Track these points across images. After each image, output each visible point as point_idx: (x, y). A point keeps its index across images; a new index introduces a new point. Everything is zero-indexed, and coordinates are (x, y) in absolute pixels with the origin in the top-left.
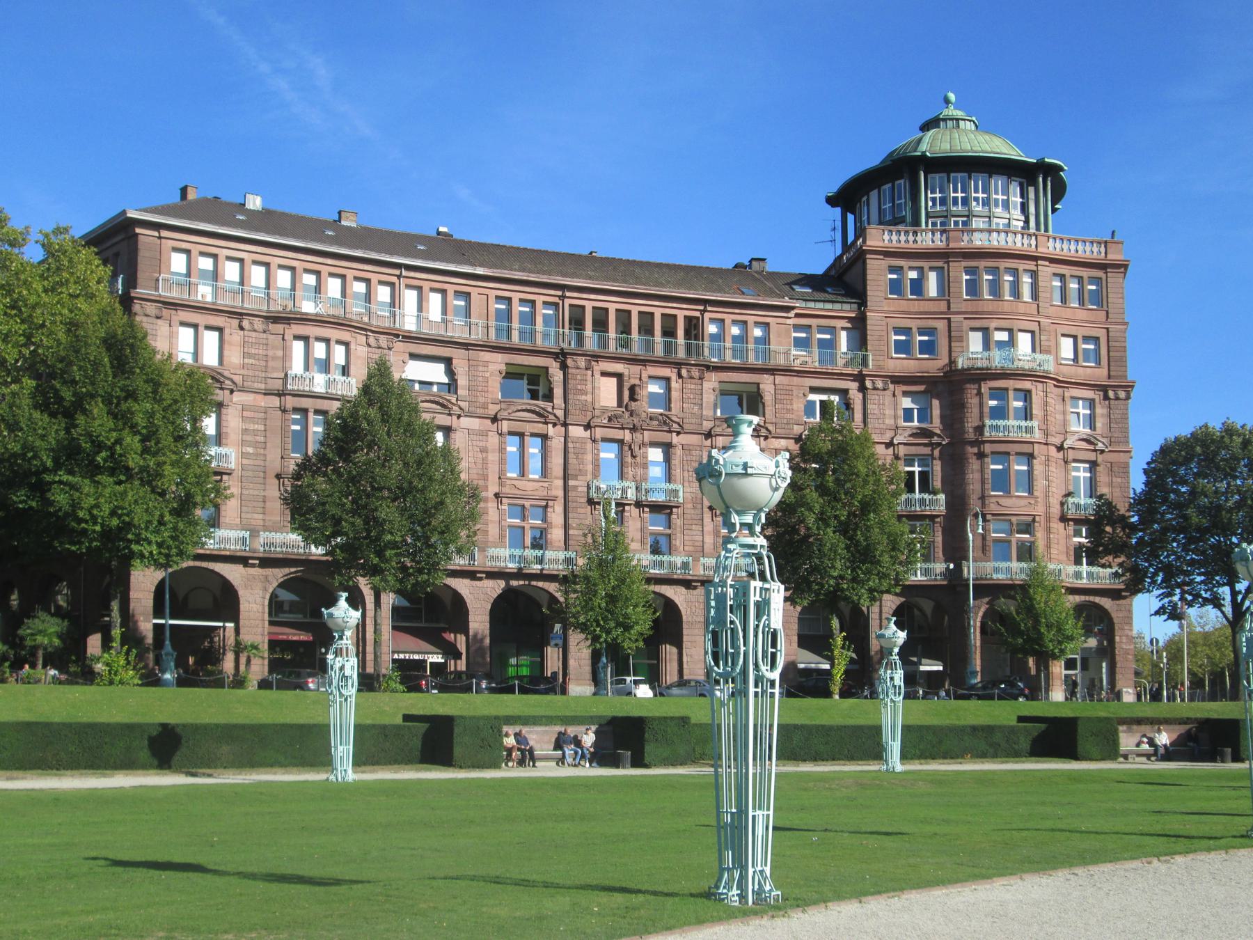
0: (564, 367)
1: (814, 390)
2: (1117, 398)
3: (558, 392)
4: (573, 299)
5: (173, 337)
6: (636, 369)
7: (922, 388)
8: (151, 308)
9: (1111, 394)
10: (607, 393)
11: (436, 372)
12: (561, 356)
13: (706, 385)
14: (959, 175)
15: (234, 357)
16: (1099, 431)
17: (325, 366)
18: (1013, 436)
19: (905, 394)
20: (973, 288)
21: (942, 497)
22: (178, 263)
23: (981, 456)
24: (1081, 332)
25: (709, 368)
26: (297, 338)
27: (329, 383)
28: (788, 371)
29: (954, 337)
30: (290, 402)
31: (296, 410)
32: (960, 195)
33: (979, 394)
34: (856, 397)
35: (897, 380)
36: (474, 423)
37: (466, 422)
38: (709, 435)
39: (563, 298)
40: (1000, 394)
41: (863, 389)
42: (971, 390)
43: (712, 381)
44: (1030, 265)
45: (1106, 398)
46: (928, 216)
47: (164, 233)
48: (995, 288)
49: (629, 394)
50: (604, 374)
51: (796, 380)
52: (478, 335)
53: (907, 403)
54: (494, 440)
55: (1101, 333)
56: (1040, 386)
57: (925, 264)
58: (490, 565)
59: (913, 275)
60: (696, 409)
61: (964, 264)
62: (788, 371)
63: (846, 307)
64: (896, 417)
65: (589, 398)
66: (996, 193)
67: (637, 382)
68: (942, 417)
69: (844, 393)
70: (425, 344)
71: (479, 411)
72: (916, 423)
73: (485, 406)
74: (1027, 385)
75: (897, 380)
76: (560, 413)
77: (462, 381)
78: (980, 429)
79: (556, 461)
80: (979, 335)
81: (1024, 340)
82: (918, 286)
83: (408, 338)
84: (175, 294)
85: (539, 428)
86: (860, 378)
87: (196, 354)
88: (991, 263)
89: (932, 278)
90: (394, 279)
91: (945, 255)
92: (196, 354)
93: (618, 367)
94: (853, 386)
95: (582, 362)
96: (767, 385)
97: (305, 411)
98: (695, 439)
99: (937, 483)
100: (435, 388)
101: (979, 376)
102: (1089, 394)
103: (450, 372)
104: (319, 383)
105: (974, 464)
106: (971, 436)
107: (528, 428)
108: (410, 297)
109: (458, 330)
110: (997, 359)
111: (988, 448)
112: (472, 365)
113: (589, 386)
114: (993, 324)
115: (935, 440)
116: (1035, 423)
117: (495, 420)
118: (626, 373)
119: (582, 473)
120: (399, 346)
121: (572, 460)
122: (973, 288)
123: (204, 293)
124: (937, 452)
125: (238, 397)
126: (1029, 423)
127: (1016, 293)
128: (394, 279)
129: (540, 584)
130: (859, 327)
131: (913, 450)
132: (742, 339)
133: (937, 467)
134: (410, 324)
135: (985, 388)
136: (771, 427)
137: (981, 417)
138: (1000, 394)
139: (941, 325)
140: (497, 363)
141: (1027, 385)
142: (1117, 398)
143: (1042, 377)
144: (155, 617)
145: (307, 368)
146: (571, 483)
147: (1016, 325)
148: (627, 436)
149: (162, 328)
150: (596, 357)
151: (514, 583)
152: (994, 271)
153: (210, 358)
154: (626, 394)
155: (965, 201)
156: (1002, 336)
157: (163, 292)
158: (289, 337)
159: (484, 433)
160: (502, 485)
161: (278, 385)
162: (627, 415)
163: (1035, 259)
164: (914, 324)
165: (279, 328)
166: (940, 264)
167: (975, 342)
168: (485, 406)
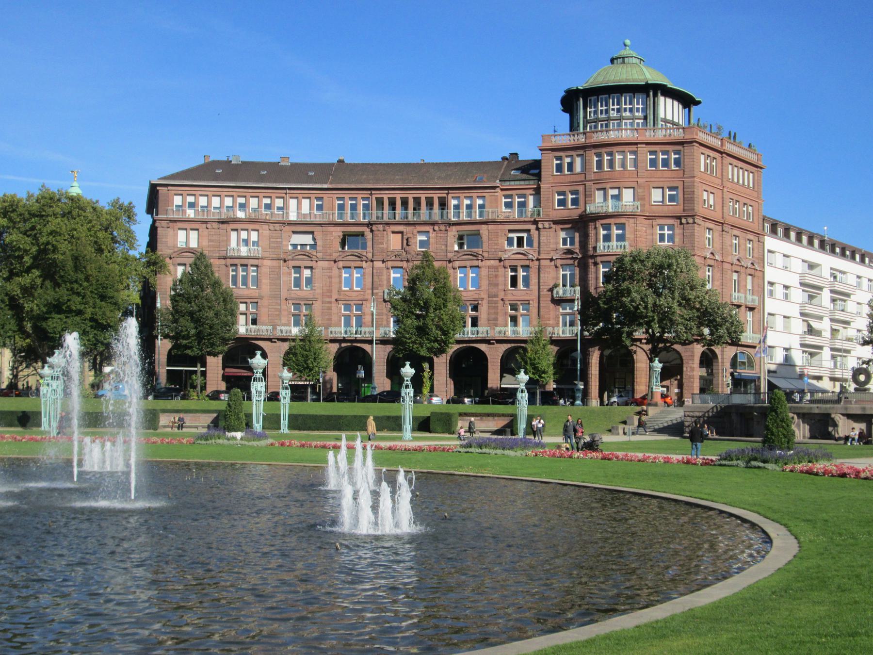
0: (372, 231)
1: (510, 231)
2: (688, 223)
3: (369, 244)
4: (377, 194)
6: (411, 228)
7: (569, 226)
8: (164, 224)
9: (684, 221)
10: (394, 242)
11: (307, 239)
12: (370, 225)
13: (449, 233)
14: (604, 96)
15: (205, 243)
16: (676, 244)
17: (246, 242)
18: (612, 251)
19: (562, 229)
20: (600, 164)
21: (578, 288)
22: (178, 200)
23: (596, 264)
24: (666, 185)
26: (233, 230)
27: (249, 251)
28: (494, 222)
29: (588, 196)
30: (229, 262)
31: (232, 265)
32: (604, 108)
33: (596, 228)
34: (534, 233)
35: (556, 222)
36: (325, 264)
37: (320, 263)
38: (450, 261)
39: (371, 194)
40: (607, 227)
41: (538, 229)
42: (591, 226)
43: (453, 232)
44: (633, 148)
45: (681, 223)
46: (586, 122)
47: (170, 188)
48: (611, 163)
50: (393, 232)
51: (500, 227)
52: (326, 219)
53: (563, 235)
54: (335, 271)
55: (680, 185)
56: (631, 221)
57: (574, 153)
59: (568, 160)
60: (443, 247)
61: (593, 151)
62: (494, 222)
63: (532, 182)
64: (557, 243)
65: (385, 246)
66: (625, 104)
67: (411, 235)
68: (580, 242)
69: (528, 231)
70: (302, 226)
71: (328, 258)
72: (568, 246)
73: (331, 255)
74: (622, 220)
75: (556, 222)
76: (370, 256)
77: (319, 243)
78: (595, 248)
79: (369, 280)
80: (602, 192)
81: (628, 195)
82: (571, 166)
83: (291, 224)
84: (176, 216)
85: (358, 264)
86: (535, 222)
87: (187, 242)
88: (609, 149)
89: (578, 161)
90: (284, 195)
91: (584, 147)
92: (187, 242)
94: (533, 227)
95: (381, 227)
97: (236, 265)
99: (577, 281)
100: (308, 248)
101: (596, 218)
102: (671, 221)
103: (314, 239)
104: (244, 251)
105: (592, 268)
106: (591, 252)
108: (293, 203)
109: (318, 216)
110: (610, 207)
111: (599, 259)
113: (385, 240)
114: (608, 186)
115: (575, 256)
116: (626, 243)
117: (335, 262)
118: (405, 231)
119: (381, 286)
120: (288, 228)
121: (376, 279)
122: (600, 164)
123: (191, 213)
124: (576, 262)
126: (623, 243)
127: (623, 165)
128: (284, 195)
129: (359, 345)
130: (537, 191)
131: (565, 262)
132: (469, 207)
133: (577, 270)
134: (293, 217)
135: (599, 223)
136: (485, 255)
137: (597, 240)
138: (607, 227)
139: (581, 189)
140: (338, 232)
141: (622, 220)
142: (688, 223)
143: (633, 216)
144: (168, 366)
145: (238, 244)
146: (375, 291)
147: (621, 185)
149: (170, 232)
150: (388, 224)
151: (343, 345)
152: (610, 154)
153: (193, 244)
154: (405, 242)
155: (607, 111)
156: (615, 192)
157: (170, 216)
158: (229, 230)
159: (330, 269)
160: (339, 294)
161: (223, 254)
162: (404, 253)
163: (636, 144)
164: (567, 189)
165: (225, 226)
166: (581, 152)
167: (599, 196)
168: (331, 255)
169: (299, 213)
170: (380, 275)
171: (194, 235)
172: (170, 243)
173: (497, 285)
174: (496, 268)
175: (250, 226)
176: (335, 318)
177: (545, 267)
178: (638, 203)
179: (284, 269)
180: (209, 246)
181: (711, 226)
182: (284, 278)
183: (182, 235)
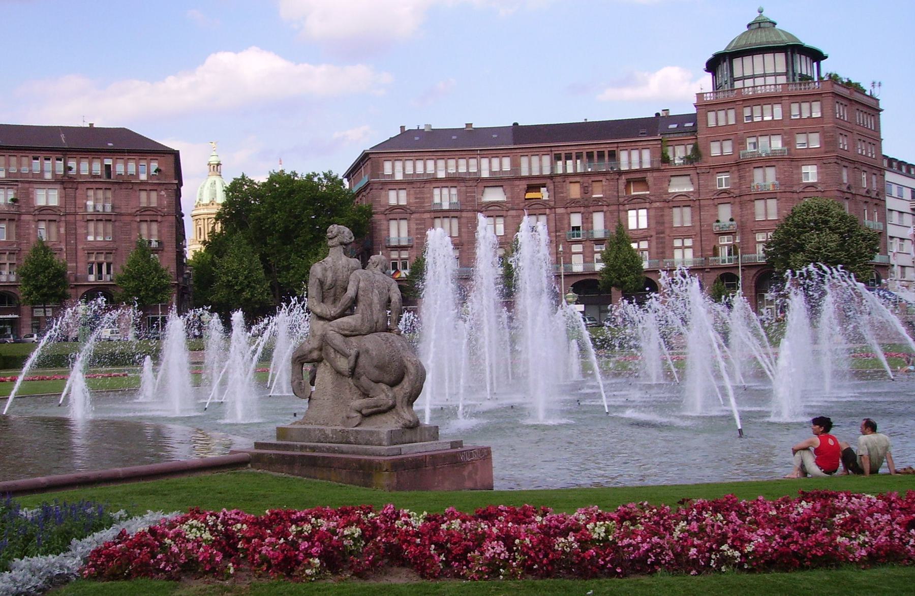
5: (388, 196)
10: (575, 191)
12: (552, 177)
13: (620, 181)
15: (412, 200)
25: (620, 173)
49: (585, 190)
60: (615, 193)
65: (564, 195)
73: (518, 204)
85: (542, 211)
93: (578, 179)
98: (615, 208)
107: (538, 212)
148: (582, 209)
149: (383, 193)
153: (403, 202)
169: (491, 172)
171: (403, 194)
172: (383, 203)
173: (663, 223)
174: (662, 209)
175: (449, 184)
177: (705, 206)
178: (786, 148)
180: (416, 203)
181: (847, 164)
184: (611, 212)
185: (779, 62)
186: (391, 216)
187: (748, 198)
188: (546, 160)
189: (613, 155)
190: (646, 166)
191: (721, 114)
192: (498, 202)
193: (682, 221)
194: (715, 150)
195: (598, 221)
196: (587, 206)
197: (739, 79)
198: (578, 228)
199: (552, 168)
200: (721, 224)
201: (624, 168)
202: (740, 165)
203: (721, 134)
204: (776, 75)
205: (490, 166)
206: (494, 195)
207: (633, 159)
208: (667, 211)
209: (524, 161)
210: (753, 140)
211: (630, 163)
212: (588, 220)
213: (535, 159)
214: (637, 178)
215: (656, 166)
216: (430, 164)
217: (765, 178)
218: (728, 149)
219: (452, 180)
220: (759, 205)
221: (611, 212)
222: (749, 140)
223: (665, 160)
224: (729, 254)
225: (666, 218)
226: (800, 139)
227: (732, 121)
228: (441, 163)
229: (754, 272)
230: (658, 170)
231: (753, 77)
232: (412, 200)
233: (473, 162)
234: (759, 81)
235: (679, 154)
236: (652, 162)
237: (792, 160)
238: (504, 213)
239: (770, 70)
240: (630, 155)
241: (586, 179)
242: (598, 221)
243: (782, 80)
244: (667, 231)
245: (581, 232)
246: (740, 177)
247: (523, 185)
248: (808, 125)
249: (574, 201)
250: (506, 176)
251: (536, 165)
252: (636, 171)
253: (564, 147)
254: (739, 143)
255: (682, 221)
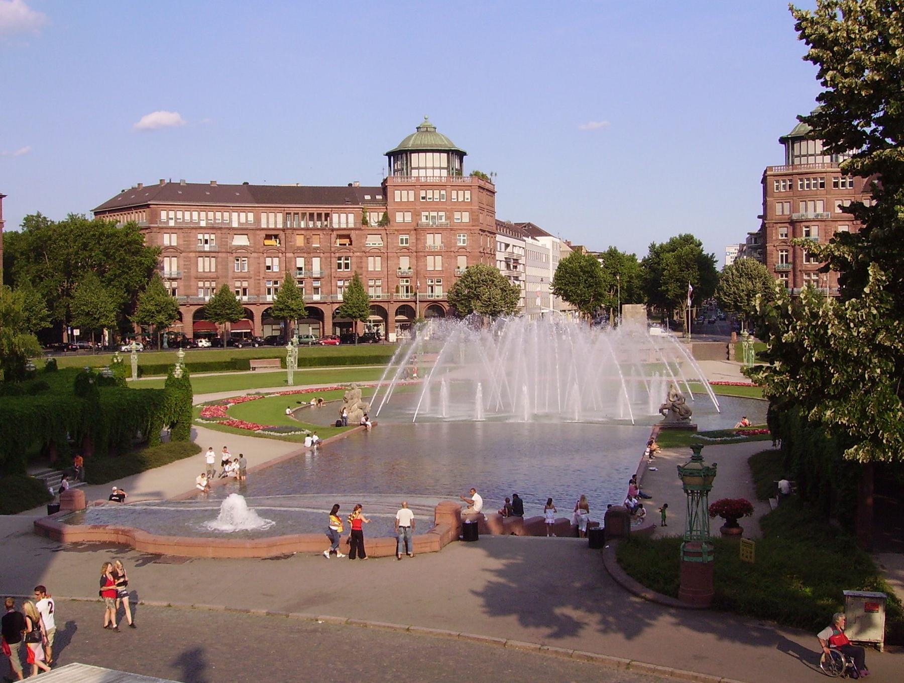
10: (300, 241)
12: (283, 230)
15: (181, 242)
25: (333, 230)
49: (308, 241)
58: (261, 301)
85: (276, 255)
93: (303, 232)
96: (353, 235)
98: (328, 255)
107: (273, 255)
112: (255, 235)
125: (183, 254)
148: (305, 255)
149: (159, 235)
153: (174, 244)
169: (239, 223)
170: (290, 262)
171: (174, 236)
174: (361, 257)
176: (262, 290)
179: (231, 258)
182: (230, 265)
183: (166, 236)
184: (326, 258)
185: (442, 159)
186: (165, 254)
187: (422, 254)
188: (280, 217)
189: (327, 215)
190: (351, 225)
191: (404, 193)
192: (245, 246)
193: (375, 267)
194: (399, 218)
195: (316, 262)
196: (308, 252)
197: (415, 168)
198: (300, 269)
199: (285, 223)
200: (402, 270)
201: (335, 226)
202: (418, 230)
203: (404, 207)
204: (441, 168)
205: (239, 219)
206: (241, 241)
207: (343, 219)
208: (364, 259)
209: (264, 216)
210: (427, 214)
211: (339, 223)
212: (308, 263)
213: (272, 215)
214: (345, 235)
215: (358, 226)
216: (195, 214)
217: (434, 241)
218: (408, 218)
219: (212, 228)
220: (430, 259)
221: (326, 258)
222: (423, 213)
223: (365, 222)
224: (407, 292)
225: (364, 265)
226: (457, 215)
227: (412, 199)
228: (203, 214)
229: (425, 304)
230: (360, 229)
231: (426, 168)
232: (181, 242)
233: (226, 215)
234: (430, 172)
235: (374, 218)
236: (355, 223)
237: (451, 230)
238: (249, 255)
239: (437, 165)
240: (339, 217)
241: (309, 232)
242: (316, 262)
243: (444, 173)
244: (364, 274)
245: (303, 271)
246: (417, 239)
247: (263, 234)
248: (461, 207)
249: (299, 248)
250: (249, 227)
251: (273, 219)
252: (345, 229)
253: (294, 208)
254: (416, 215)
255: (375, 267)
